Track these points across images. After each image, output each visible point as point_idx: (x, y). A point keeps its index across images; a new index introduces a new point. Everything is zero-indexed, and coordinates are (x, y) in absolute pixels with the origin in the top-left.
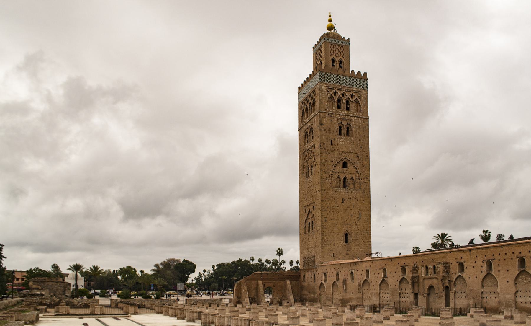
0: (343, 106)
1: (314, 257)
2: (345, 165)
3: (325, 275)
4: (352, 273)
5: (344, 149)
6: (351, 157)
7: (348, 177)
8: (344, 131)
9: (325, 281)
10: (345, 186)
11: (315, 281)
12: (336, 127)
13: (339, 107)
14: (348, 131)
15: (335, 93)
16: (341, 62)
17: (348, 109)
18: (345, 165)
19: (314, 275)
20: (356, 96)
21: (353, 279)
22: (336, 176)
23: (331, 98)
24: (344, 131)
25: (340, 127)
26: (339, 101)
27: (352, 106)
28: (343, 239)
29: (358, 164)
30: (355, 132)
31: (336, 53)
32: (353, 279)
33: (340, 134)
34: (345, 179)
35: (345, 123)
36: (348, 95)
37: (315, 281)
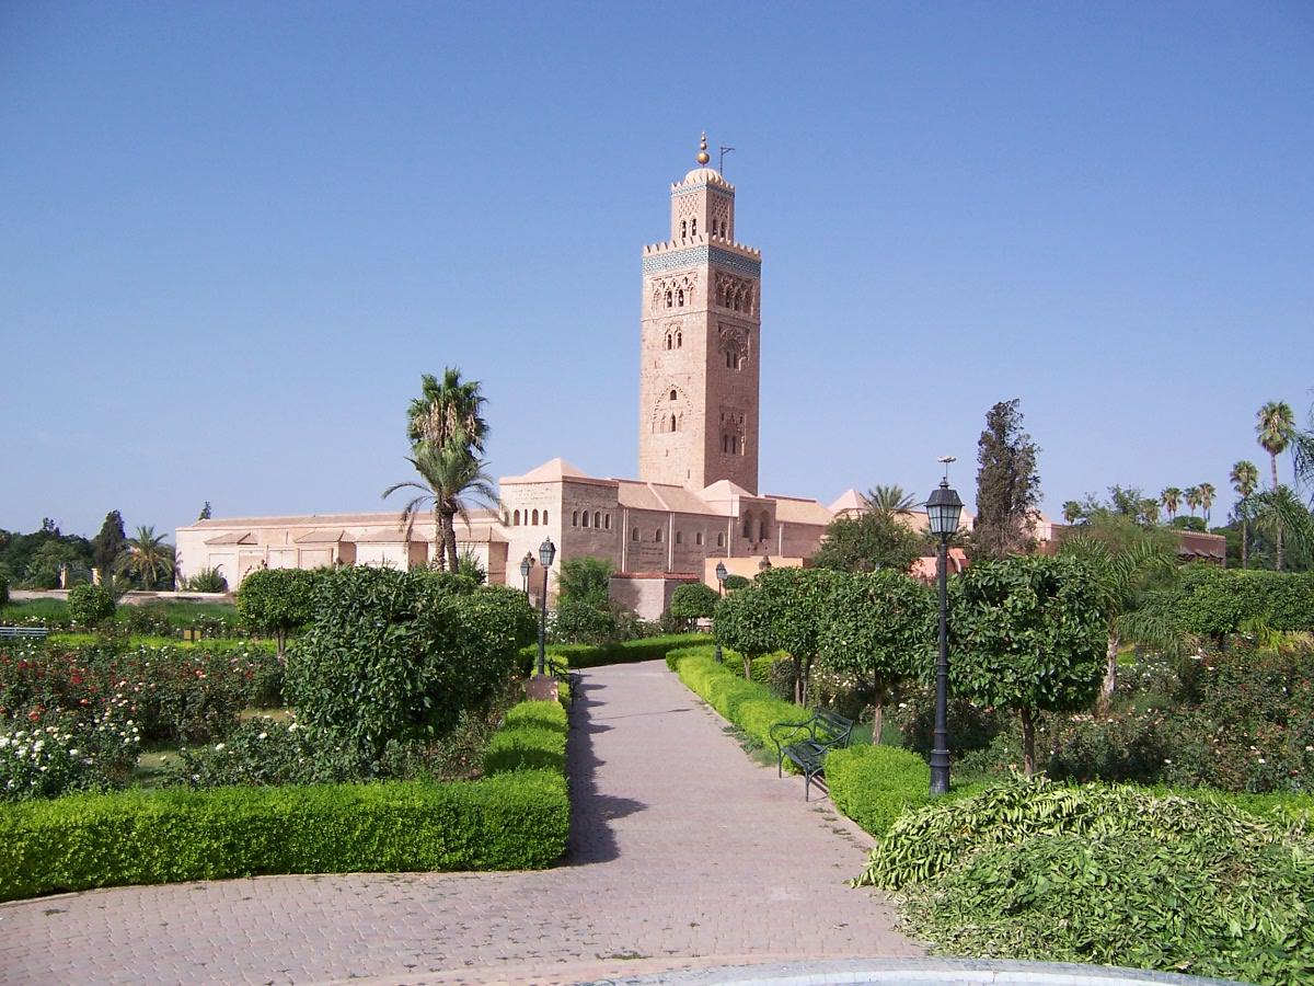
0: (675, 300)
2: (673, 395)
5: (671, 371)
6: (678, 383)
8: (675, 341)
10: (674, 430)
12: (662, 337)
18: (673, 395)
23: (657, 294)
24: (675, 341)
25: (670, 336)
26: (670, 294)
30: (687, 339)
31: (686, 209)
33: (670, 348)
34: (674, 417)
35: (674, 328)
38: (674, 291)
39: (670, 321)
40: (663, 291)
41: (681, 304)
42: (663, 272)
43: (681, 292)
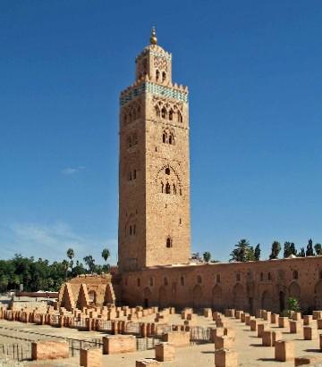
0: (167, 116)
1: (137, 259)
2: (168, 172)
3: (151, 279)
4: (182, 278)
6: (173, 164)
7: (171, 183)
8: (167, 139)
9: (152, 285)
11: (139, 285)
13: (163, 117)
14: (170, 139)
15: (160, 103)
16: (164, 74)
17: (171, 119)
18: (168, 172)
19: (139, 280)
20: (179, 107)
21: (183, 283)
22: (159, 182)
23: (156, 107)
24: (167, 139)
26: (164, 110)
27: (175, 117)
28: (165, 243)
29: (178, 169)
32: (183, 283)
33: (164, 141)
34: (168, 184)
36: (172, 106)
37: (139, 285)
38: (168, 110)
39: (166, 126)
40: (161, 108)
41: (171, 119)
42: (158, 94)
43: (171, 112)
